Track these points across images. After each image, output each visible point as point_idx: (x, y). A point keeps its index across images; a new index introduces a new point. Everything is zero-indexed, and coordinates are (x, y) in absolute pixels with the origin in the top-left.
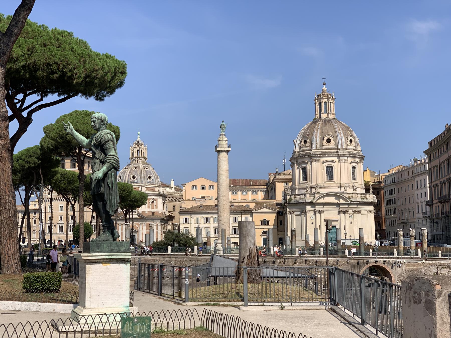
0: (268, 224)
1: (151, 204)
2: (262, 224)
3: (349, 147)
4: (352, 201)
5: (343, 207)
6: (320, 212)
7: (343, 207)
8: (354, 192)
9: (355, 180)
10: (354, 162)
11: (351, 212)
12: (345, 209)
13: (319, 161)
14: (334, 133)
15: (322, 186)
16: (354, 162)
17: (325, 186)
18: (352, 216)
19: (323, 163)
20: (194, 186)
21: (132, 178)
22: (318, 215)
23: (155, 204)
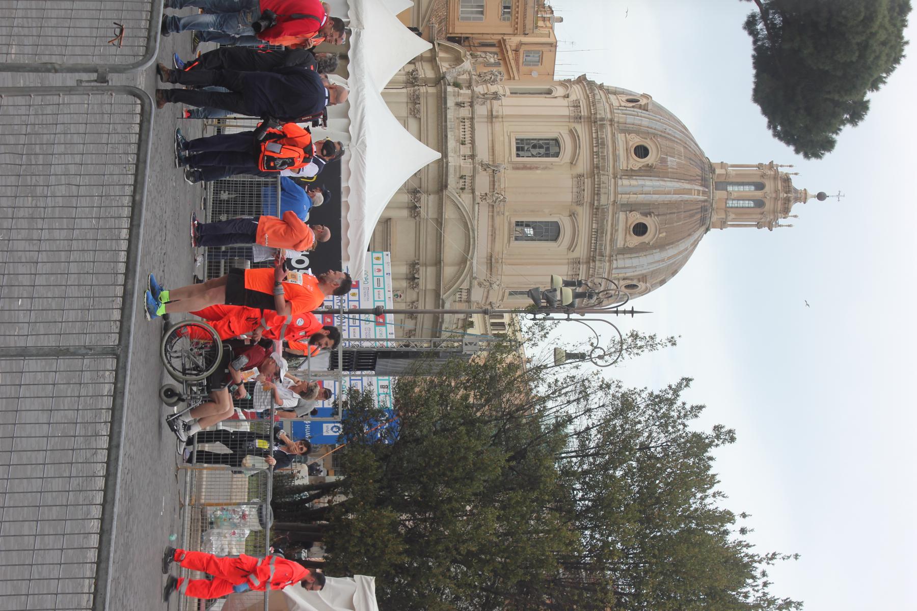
12: (421, 282)
13: (579, 203)
17: (498, 220)
19: (572, 215)
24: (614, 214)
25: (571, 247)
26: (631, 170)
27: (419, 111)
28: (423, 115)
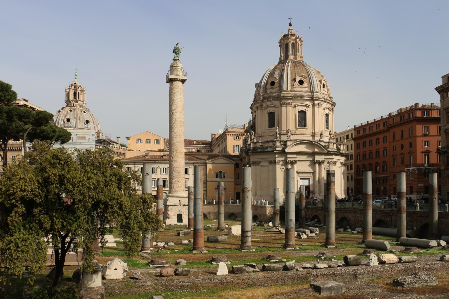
0: (224, 177)
2: (217, 177)
3: (322, 92)
4: (329, 151)
5: (318, 158)
6: (293, 163)
7: (318, 158)
14: (306, 75)
15: (294, 133)
17: (297, 133)
19: (295, 107)
24: (295, 91)
25: (307, 106)
26: (279, 86)
27: (258, 162)
28: (259, 160)
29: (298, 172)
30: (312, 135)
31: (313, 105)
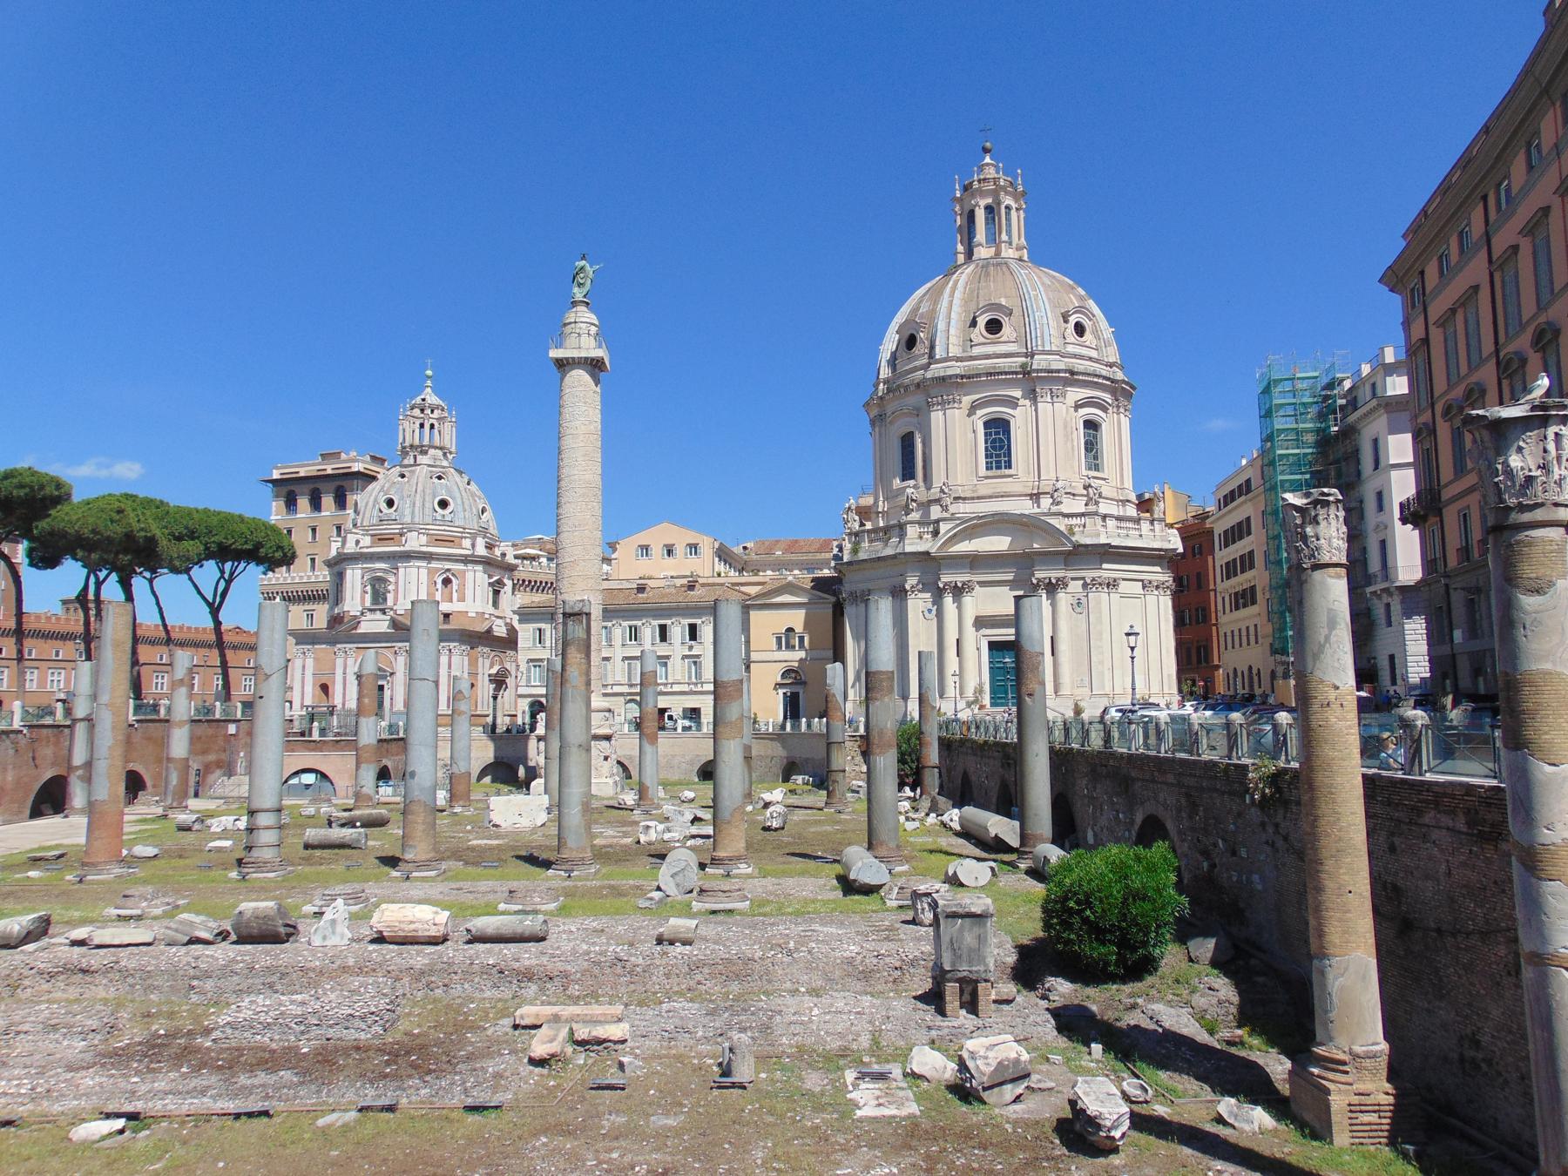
1: (439, 585)
2: (780, 648)
3: (1070, 349)
8: (1092, 508)
9: (1097, 468)
10: (1089, 403)
11: (1075, 586)
16: (1089, 403)
18: (1084, 600)
20: (645, 549)
21: (384, 506)
22: (948, 600)
23: (455, 587)
25: (1012, 403)
29: (980, 623)
30: (1031, 495)
31: (1032, 395)
